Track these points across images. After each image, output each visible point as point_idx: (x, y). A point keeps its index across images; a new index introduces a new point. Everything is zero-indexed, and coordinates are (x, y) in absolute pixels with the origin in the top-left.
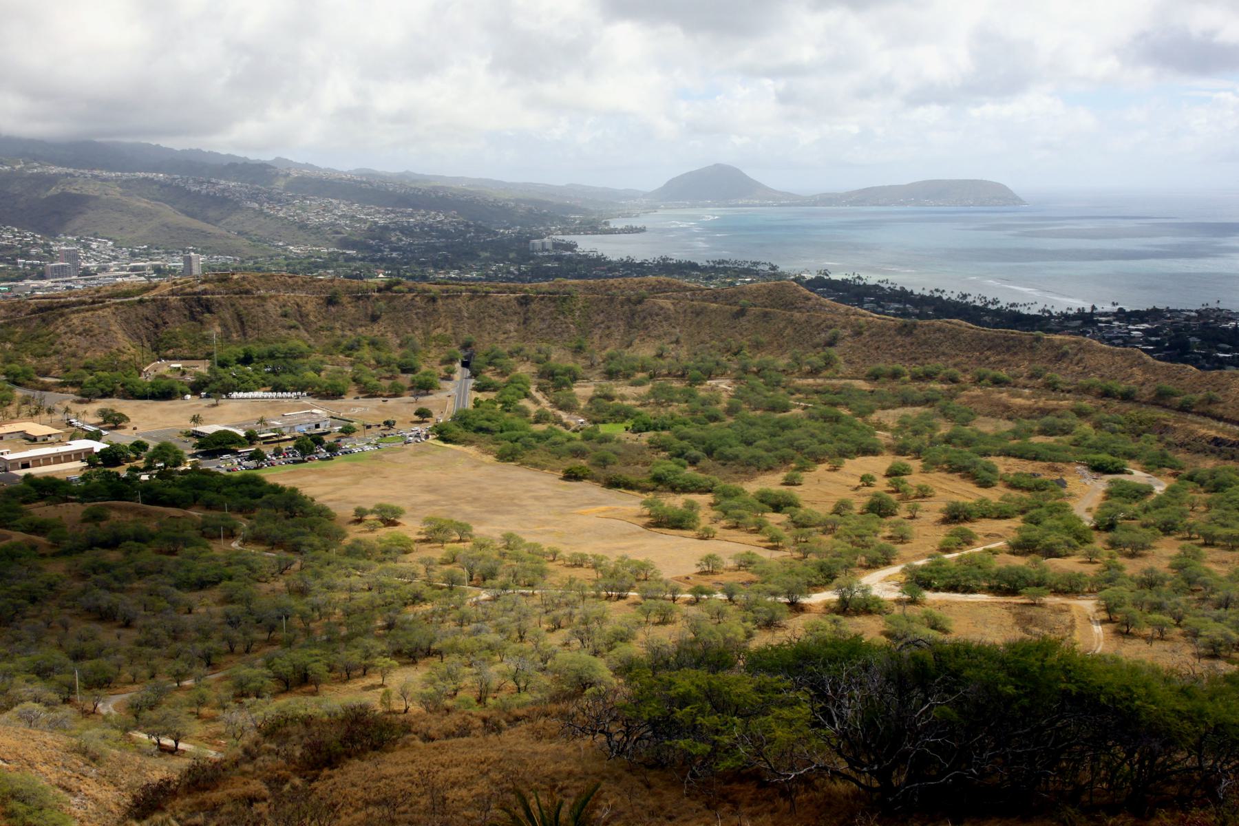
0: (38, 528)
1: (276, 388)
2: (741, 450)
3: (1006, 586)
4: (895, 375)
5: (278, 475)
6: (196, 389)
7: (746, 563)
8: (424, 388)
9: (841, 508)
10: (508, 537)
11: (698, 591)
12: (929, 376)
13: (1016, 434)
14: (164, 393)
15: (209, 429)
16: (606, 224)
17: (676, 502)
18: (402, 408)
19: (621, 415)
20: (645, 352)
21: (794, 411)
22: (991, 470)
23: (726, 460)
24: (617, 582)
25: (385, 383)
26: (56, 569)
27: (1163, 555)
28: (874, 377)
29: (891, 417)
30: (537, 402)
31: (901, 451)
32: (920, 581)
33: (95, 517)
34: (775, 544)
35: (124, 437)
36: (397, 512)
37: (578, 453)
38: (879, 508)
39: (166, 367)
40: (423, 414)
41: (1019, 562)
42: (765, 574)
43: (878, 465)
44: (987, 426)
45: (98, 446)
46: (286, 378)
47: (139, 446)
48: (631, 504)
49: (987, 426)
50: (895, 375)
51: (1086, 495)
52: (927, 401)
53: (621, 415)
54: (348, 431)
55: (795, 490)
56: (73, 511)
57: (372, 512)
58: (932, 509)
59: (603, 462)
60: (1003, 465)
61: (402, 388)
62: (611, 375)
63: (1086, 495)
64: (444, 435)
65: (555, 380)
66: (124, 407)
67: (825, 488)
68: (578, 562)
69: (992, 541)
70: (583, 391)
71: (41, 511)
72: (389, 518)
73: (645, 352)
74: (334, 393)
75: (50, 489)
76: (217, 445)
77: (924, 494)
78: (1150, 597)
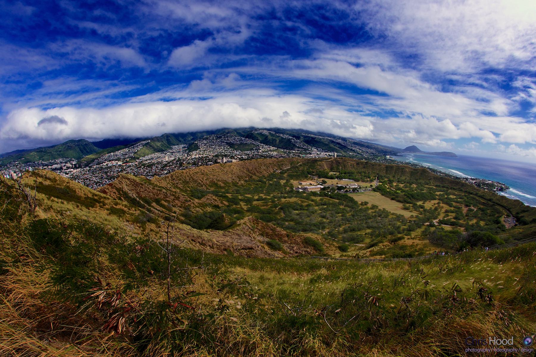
0: (313, 201)
1: (350, 179)
2: (417, 197)
3: (452, 224)
4: (439, 186)
5: (349, 195)
6: (337, 178)
7: (417, 217)
8: (371, 181)
9: (431, 208)
10: (384, 209)
11: (410, 221)
12: (443, 187)
13: (456, 198)
14: (332, 178)
15: (339, 185)
17: (408, 205)
18: (368, 185)
19: (399, 189)
20: (403, 178)
22: (452, 204)
23: (414, 198)
26: (316, 208)
27: (474, 221)
28: (436, 186)
29: (438, 193)
31: (439, 199)
33: (321, 200)
34: (421, 214)
35: (326, 185)
36: (368, 203)
37: (393, 195)
38: (436, 209)
39: (331, 173)
40: (371, 186)
41: (455, 220)
42: (420, 219)
44: (451, 196)
45: (322, 187)
46: (351, 177)
47: (329, 187)
48: (401, 205)
49: (451, 196)
50: (439, 186)
53: (399, 189)
54: (360, 188)
56: (318, 198)
58: (443, 210)
59: (397, 197)
60: (454, 204)
62: (398, 182)
63: (465, 210)
64: (374, 190)
65: (390, 182)
66: (326, 180)
68: (393, 214)
69: (451, 216)
70: (395, 184)
71: (313, 198)
72: (366, 203)
73: (403, 178)
74: (357, 180)
75: (314, 194)
76: (340, 188)
77: (442, 207)
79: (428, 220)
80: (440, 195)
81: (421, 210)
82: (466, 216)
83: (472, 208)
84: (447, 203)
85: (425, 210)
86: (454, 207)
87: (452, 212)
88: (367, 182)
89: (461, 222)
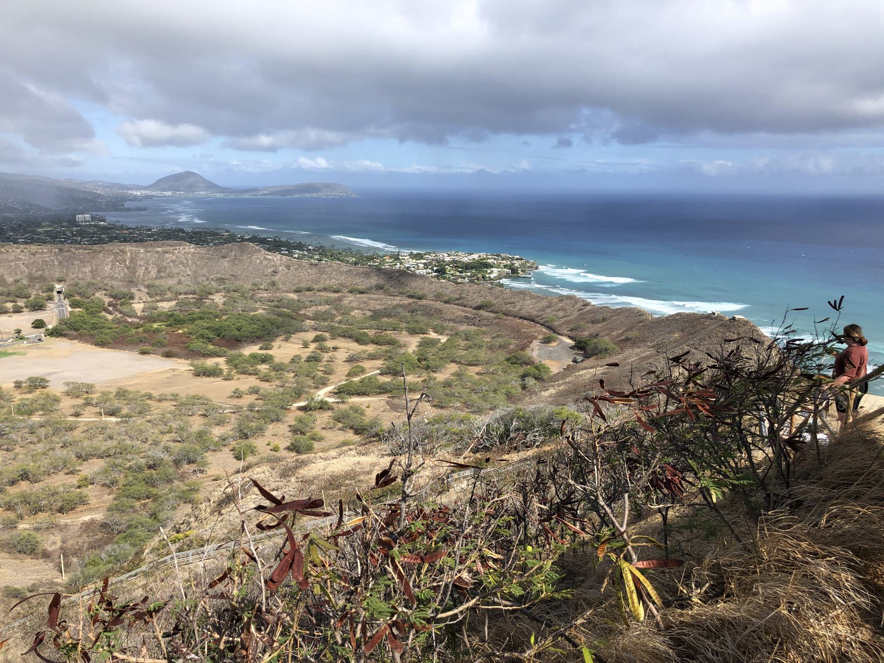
16: (123, 205)
21: (260, 311)
22: (366, 335)
24: (186, 406)
25: (9, 305)
30: (110, 313)
32: (340, 392)
34: (266, 379)
36: (43, 380)
41: (387, 379)
43: (311, 335)
48: (182, 366)
51: (412, 344)
52: (327, 303)
55: (269, 352)
57: (25, 383)
58: (341, 355)
61: (22, 308)
63: (412, 344)
67: (284, 350)
69: (372, 369)
72: (37, 383)
78: (448, 390)
79: (298, 394)
80: (316, 317)
81: (263, 368)
82: (419, 360)
83: (433, 335)
84: (347, 335)
85: (279, 368)
86: (373, 342)
87: (372, 357)
88: (18, 310)
89: (410, 378)
